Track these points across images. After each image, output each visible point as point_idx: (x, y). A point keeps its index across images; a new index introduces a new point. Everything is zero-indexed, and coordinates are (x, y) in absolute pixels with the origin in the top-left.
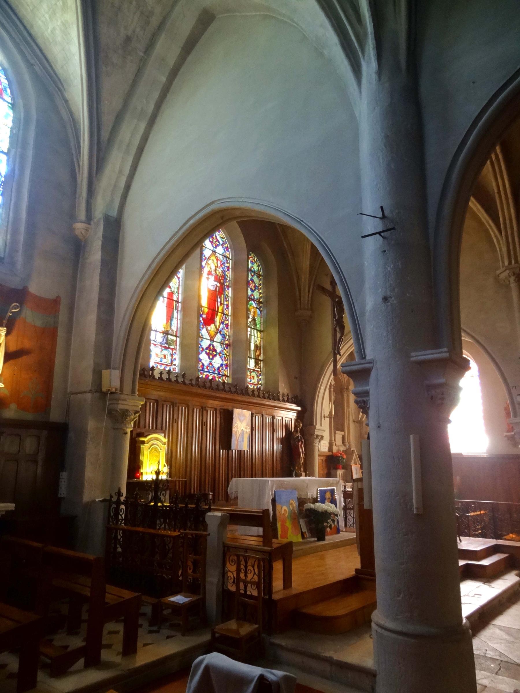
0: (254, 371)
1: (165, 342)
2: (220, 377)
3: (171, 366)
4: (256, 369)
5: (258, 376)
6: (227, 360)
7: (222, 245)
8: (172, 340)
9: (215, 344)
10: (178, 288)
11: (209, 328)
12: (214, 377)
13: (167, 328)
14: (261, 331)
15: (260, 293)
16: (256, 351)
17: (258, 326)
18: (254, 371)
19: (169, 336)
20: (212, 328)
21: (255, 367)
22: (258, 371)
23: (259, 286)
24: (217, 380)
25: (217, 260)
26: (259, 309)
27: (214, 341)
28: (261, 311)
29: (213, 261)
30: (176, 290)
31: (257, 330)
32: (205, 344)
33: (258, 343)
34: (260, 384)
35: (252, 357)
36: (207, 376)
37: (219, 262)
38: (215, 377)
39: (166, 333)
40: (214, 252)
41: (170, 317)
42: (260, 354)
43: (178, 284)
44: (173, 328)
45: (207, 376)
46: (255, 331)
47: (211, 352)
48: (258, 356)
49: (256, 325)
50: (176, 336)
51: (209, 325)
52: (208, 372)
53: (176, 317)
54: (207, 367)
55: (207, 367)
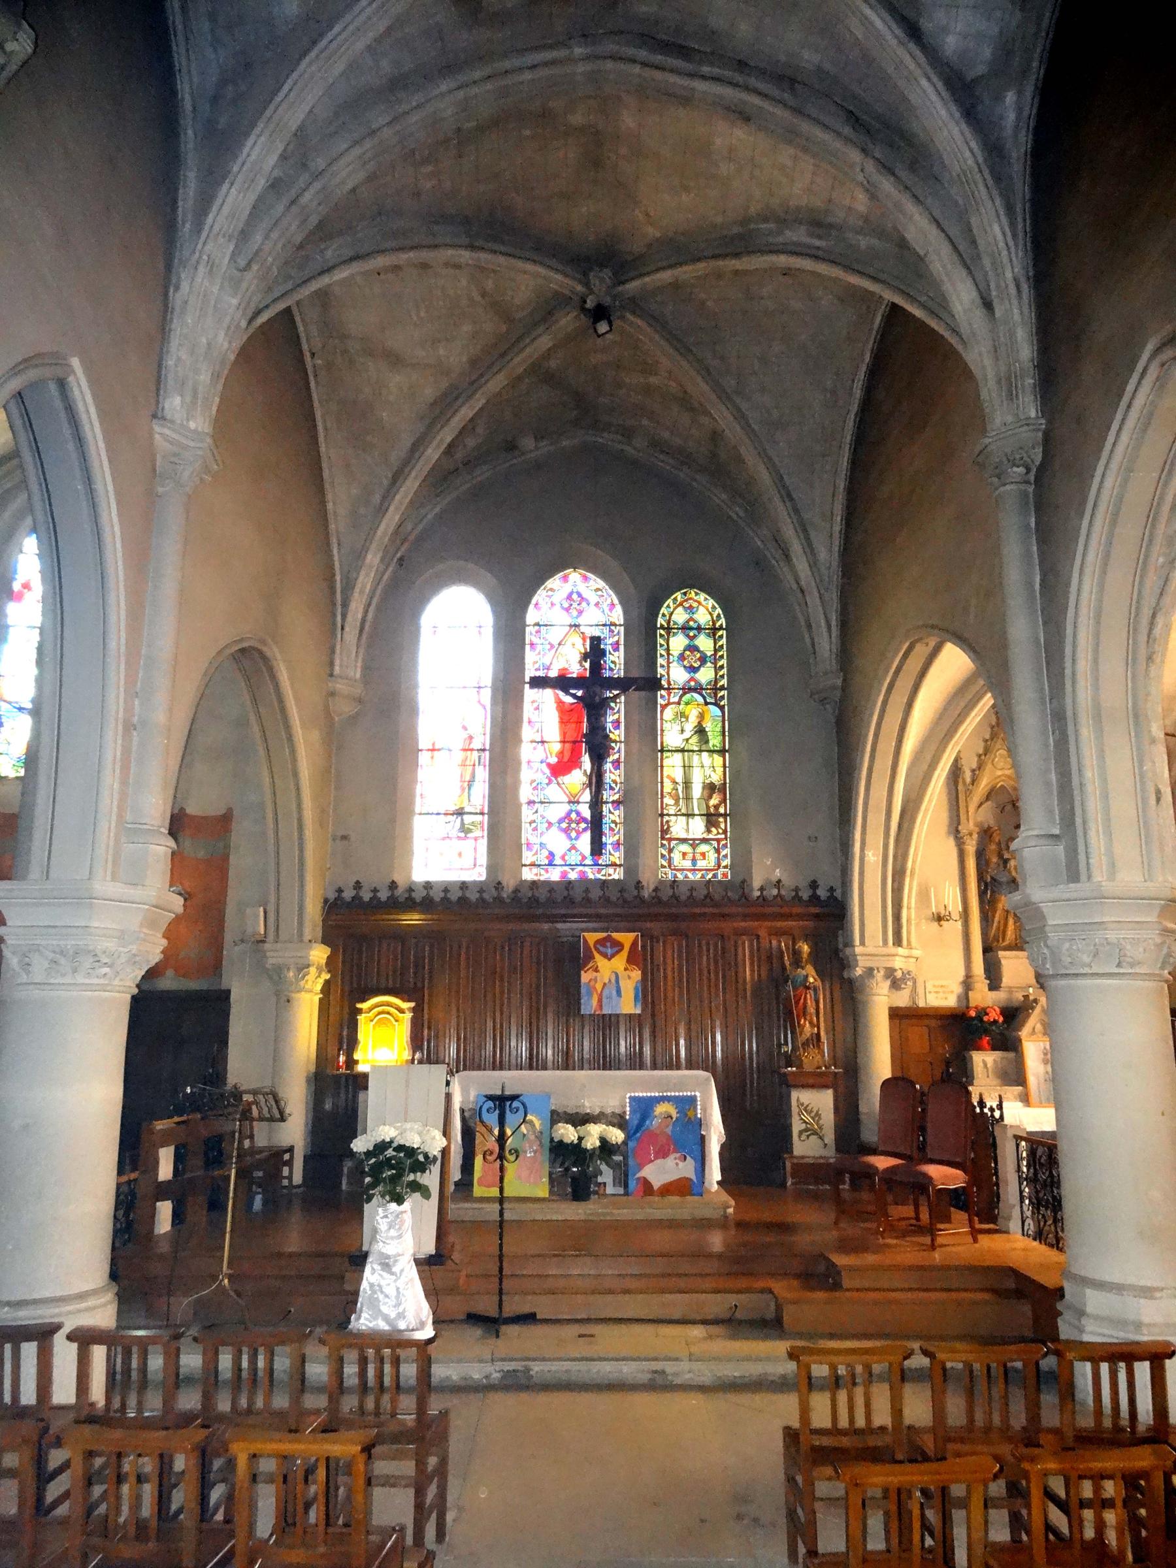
0: (705, 841)
2: (599, 871)
4: (711, 836)
5: (718, 851)
6: (619, 832)
7: (597, 604)
12: (583, 873)
14: (722, 752)
16: (710, 797)
17: (715, 741)
18: (705, 841)
20: (577, 779)
22: (718, 841)
23: (715, 654)
26: (716, 704)
28: (722, 708)
31: (711, 751)
33: (716, 778)
34: (725, 867)
39: (460, 813)
42: (724, 801)
47: (574, 825)
48: (716, 807)
49: (707, 742)
50: (482, 814)
54: (563, 858)
55: (563, 858)
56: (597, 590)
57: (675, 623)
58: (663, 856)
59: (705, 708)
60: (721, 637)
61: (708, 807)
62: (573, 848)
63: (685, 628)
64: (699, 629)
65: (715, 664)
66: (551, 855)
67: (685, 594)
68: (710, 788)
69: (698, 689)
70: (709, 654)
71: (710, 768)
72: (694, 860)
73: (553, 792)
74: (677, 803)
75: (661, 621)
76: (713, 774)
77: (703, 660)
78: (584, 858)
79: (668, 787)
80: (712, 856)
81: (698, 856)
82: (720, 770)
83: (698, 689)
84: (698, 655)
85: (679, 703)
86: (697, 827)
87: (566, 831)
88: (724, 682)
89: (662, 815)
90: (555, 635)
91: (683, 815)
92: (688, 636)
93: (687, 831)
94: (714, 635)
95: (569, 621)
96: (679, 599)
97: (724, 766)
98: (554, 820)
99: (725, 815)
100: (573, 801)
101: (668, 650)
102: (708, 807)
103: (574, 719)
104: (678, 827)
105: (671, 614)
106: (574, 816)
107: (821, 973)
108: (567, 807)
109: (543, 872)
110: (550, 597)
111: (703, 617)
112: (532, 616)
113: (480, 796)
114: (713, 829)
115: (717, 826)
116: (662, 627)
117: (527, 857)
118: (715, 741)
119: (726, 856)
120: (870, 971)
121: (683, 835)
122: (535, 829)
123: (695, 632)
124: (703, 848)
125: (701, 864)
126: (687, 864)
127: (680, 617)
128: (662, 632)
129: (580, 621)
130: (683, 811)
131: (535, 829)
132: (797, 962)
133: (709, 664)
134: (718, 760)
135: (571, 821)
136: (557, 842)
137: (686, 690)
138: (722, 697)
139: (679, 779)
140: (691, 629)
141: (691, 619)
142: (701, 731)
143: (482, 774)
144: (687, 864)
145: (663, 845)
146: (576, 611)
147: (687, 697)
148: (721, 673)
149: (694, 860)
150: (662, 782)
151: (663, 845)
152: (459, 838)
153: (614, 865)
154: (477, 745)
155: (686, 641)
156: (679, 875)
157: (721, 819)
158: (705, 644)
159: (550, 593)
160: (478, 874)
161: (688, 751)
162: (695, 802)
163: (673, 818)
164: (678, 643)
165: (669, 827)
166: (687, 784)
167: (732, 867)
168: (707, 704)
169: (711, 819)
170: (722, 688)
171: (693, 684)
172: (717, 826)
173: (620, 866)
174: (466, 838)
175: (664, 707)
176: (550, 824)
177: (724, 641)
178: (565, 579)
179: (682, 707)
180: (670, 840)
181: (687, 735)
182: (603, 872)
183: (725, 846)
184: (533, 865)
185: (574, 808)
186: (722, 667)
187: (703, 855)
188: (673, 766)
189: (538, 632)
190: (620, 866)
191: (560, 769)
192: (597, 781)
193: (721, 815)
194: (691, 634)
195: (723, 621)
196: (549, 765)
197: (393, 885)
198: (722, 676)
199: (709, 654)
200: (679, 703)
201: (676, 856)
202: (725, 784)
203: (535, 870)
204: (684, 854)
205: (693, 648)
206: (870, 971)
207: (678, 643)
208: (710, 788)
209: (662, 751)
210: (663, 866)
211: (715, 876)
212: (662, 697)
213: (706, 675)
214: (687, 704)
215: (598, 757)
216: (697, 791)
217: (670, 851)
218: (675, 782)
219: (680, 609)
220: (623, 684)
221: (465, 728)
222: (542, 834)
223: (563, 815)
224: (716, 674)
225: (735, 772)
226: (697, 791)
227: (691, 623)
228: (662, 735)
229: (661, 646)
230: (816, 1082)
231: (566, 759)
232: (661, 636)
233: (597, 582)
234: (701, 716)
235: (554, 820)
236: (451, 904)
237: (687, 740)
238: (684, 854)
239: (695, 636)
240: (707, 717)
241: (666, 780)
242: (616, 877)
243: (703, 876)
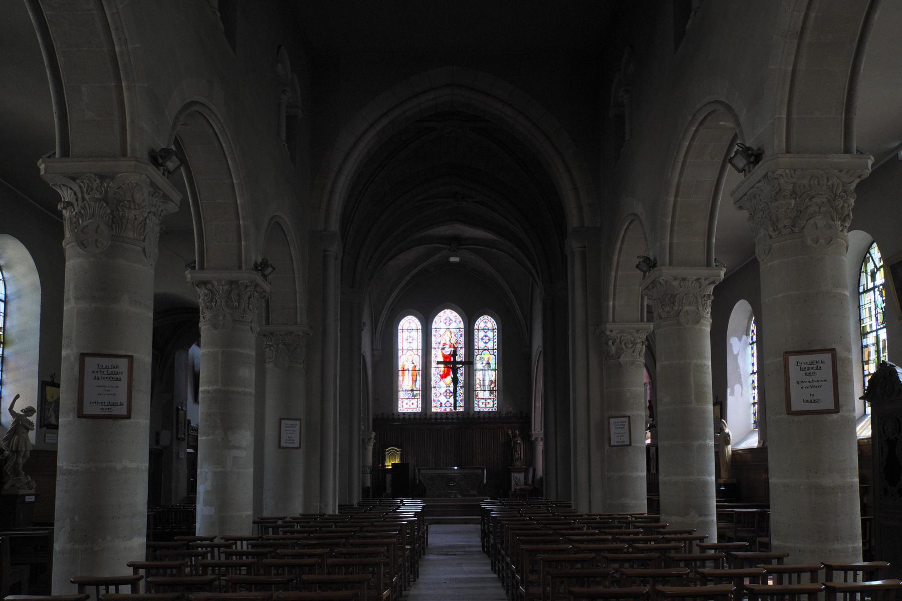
20: (449, 379)
32: (443, 390)
39: (412, 390)
41: (414, 381)
68: (491, 382)
69: (488, 350)
71: (491, 376)
73: (442, 384)
75: (476, 327)
79: (478, 382)
80: (491, 403)
83: (488, 350)
86: (487, 394)
90: (442, 332)
107: (522, 439)
111: (489, 325)
112: (434, 326)
113: (419, 385)
117: (433, 404)
118: (493, 366)
120: (536, 439)
127: (482, 325)
132: (515, 436)
134: (494, 373)
136: (443, 399)
142: (488, 363)
143: (419, 378)
146: (448, 324)
154: (417, 368)
158: (490, 334)
160: (419, 410)
164: (481, 334)
169: (491, 391)
188: (479, 375)
191: (443, 376)
192: (455, 381)
197: (393, 414)
201: (480, 404)
206: (536, 439)
207: (481, 334)
208: (491, 382)
215: (455, 373)
216: (487, 383)
220: (461, 363)
225: (498, 376)
230: (519, 471)
236: (410, 418)
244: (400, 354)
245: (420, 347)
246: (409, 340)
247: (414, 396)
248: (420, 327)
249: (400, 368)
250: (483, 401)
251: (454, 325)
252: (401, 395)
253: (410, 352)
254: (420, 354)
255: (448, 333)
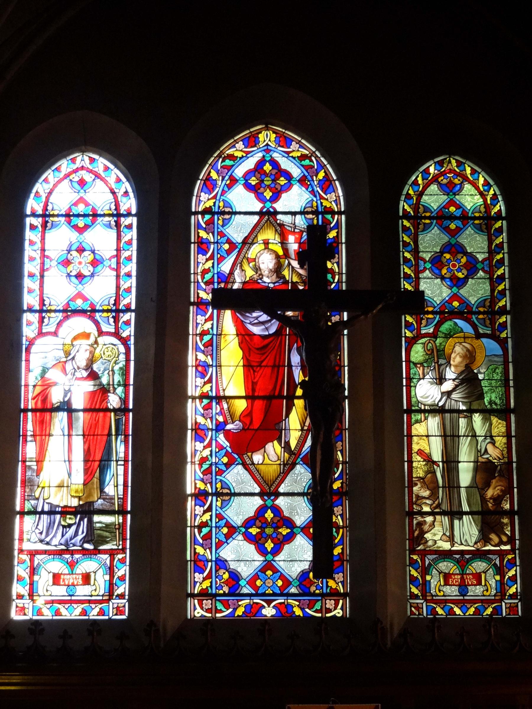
0: (479, 555)
1: (80, 537)
3: (107, 601)
4: (489, 547)
5: (500, 571)
6: (341, 542)
8: (108, 527)
9: (281, 502)
10: (125, 371)
11: (257, 458)
13: (90, 495)
14: (503, 413)
15: (494, 282)
16: (488, 485)
18: (479, 555)
19: (96, 518)
21: (484, 538)
22: (502, 554)
23: (490, 258)
24: (298, 612)
25: (283, 232)
26: (493, 337)
27: (277, 494)
28: (503, 343)
29: (266, 243)
30: (117, 378)
31: (487, 413)
32: (242, 509)
33: (494, 453)
34: (513, 596)
35: (466, 508)
36: (253, 610)
37: (291, 239)
38: (289, 607)
39: (86, 511)
40: (268, 216)
41: (97, 464)
42: (509, 490)
43: (122, 357)
44: (110, 490)
45: (253, 610)
46: (477, 418)
47: (269, 531)
48: (498, 500)
49: (481, 396)
50: (122, 512)
51: (260, 446)
52: (257, 595)
53: (122, 455)
55: (251, 582)
56: (303, 157)
57: (426, 209)
58: (413, 580)
59: (476, 343)
60: (500, 231)
61: (483, 500)
62: (268, 566)
63: (441, 217)
64: (465, 217)
65: (490, 273)
66: (235, 577)
67: (441, 163)
68: (485, 470)
69: (465, 312)
70: (480, 257)
71: (485, 437)
72: (463, 587)
74: (434, 495)
76: (490, 448)
77: (472, 267)
78: (287, 583)
79: (419, 467)
80: (492, 580)
81: (469, 580)
82: (500, 441)
84: (464, 260)
85: (434, 336)
86: (468, 531)
87: (257, 542)
88: (505, 302)
89: (411, 514)
91: (443, 513)
92: (447, 229)
93: (451, 539)
94: (489, 227)
95: (257, 206)
96: (432, 170)
97: (508, 435)
98: (238, 520)
99: (511, 513)
100: (269, 490)
101: (416, 252)
102: (483, 500)
103: (269, 361)
104: (436, 536)
105: (420, 195)
106: (269, 515)
108: (258, 502)
109: (220, 606)
110: (229, 168)
111: (470, 199)
112: (202, 200)
113: (116, 482)
114: (494, 538)
115: (499, 530)
116: (406, 216)
117: (199, 581)
119: (513, 579)
121: (446, 546)
122: (208, 537)
123: (459, 223)
124: (479, 566)
125: (475, 591)
126: (452, 591)
127: (434, 199)
128: (406, 223)
129: (279, 206)
130: (445, 507)
131: (208, 537)
133: (481, 273)
134: (498, 426)
135: (265, 524)
136: (242, 556)
137: (445, 313)
138: (503, 326)
139: (437, 456)
140: (452, 218)
141: (452, 203)
144: (452, 591)
145: (413, 563)
147: (446, 326)
148: (501, 287)
149: (463, 587)
150: (410, 462)
151: (413, 563)
152: (85, 552)
153: (334, 594)
155: (445, 238)
156: (439, 611)
157: (505, 521)
159: (228, 162)
160: (117, 610)
161: (451, 411)
162: (463, 492)
163: (429, 519)
164: (431, 241)
165: (423, 533)
166: (451, 461)
167: (524, 596)
168: (478, 336)
170: (503, 311)
171: (456, 304)
172: (499, 530)
173: (344, 596)
174: (96, 551)
175: (411, 342)
176: (232, 530)
177: (503, 238)
178: (252, 141)
179: (438, 341)
180: (424, 554)
181: (448, 386)
182: (318, 606)
183: (512, 564)
184: (204, 594)
185: (269, 503)
186: (501, 278)
187: (478, 577)
188: (426, 436)
189: (210, 222)
190: (344, 596)
193: (505, 513)
194: (453, 226)
195: (500, 206)
196: (228, 435)
198: (503, 293)
199: (480, 257)
200: (434, 336)
201: (434, 580)
202: (510, 462)
203: (207, 603)
204: (447, 577)
205: (455, 249)
207: (431, 241)
209: (410, 411)
210: (414, 596)
211: (497, 610)
212: (408, 325)
213: (476, 291)
214: (448, 336)
216: (465, 476)
217: (425, 571)
218: (428, 459)
219: (434, 187)
221: (93, 376)
222: (219, 544)
223: (251, 513)
224: (493, 290)
226: (465, 476)
227: (452, 209)
228: (409, 387)
229: (406, 244)
231: (256, 425)
232: (405, 229)
233: (301, 146)
234: (470, 357)
235: (238, 520)
237: (449, 394)
238: (447, 577)
239: (459, 229)
240: (480, 357)
241: (416, 458)
242: (338, 613)
243: (477, 611)
244: (28, 331)
245: (130, 299)
246: (81, 264)
247: (95, 538)
248: (130, 203)
249: (28, 397)
250: (445, 566)
251: (295, 199)
252: (28, 532)
253: (81, 324)
254: (128, 332)
255: (270, 235)
